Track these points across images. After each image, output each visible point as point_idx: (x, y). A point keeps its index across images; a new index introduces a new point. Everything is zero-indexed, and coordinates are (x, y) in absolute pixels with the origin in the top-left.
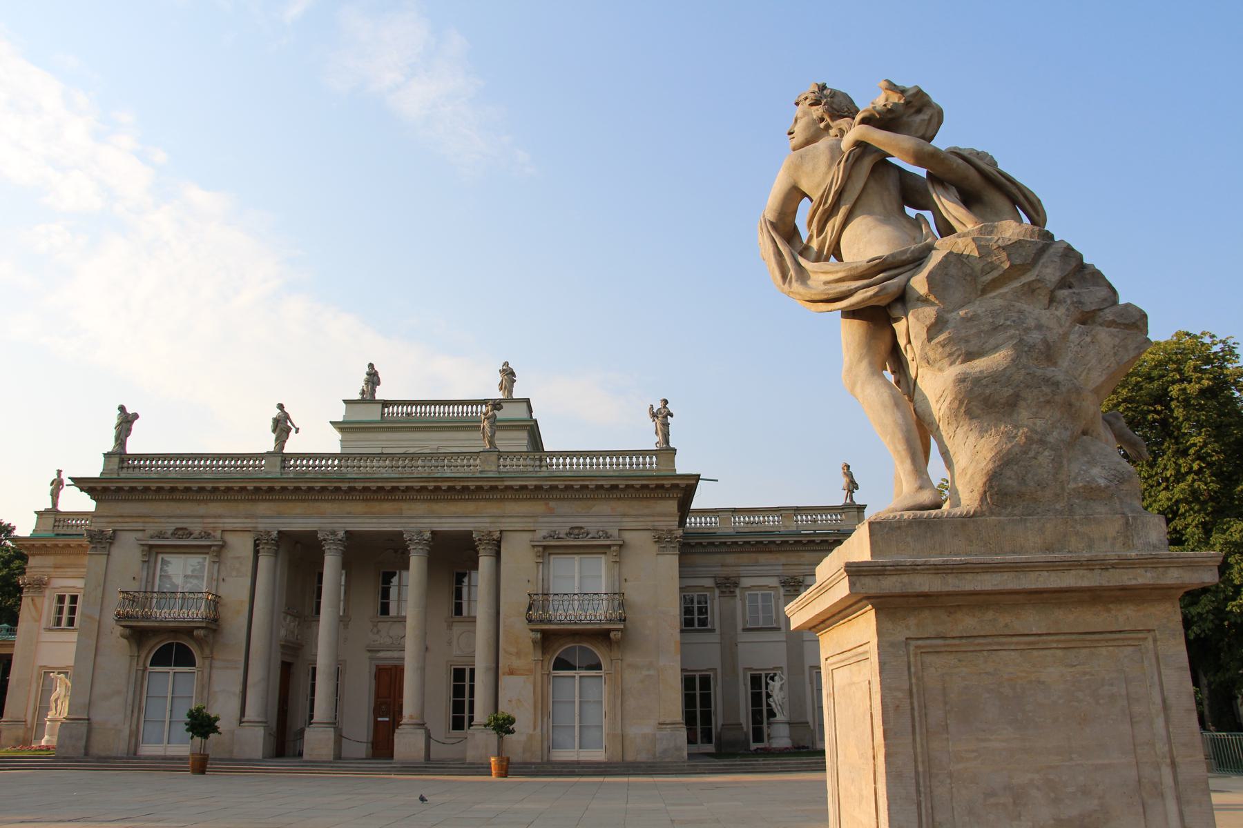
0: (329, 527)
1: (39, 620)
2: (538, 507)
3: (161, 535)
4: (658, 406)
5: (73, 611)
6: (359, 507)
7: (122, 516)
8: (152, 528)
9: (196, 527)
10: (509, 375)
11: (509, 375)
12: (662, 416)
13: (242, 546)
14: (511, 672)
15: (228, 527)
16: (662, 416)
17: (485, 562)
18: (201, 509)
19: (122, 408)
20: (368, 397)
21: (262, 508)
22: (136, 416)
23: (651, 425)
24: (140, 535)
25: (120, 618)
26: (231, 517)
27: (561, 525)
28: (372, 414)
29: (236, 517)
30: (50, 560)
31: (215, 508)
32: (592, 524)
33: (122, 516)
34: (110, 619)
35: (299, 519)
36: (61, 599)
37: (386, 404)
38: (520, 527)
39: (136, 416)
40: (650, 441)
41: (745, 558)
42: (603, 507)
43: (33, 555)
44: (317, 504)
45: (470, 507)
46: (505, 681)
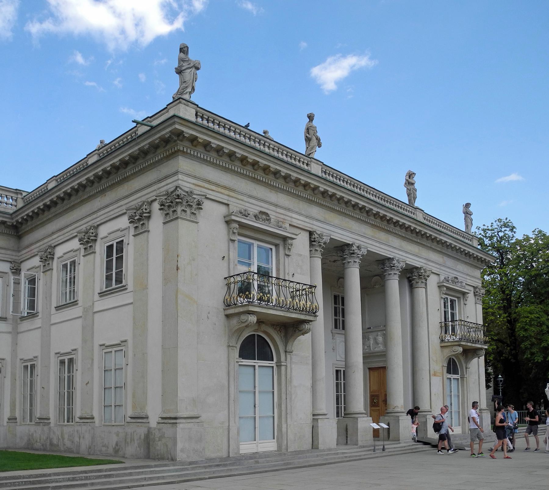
0: (357, 243)
3: (246, 215)
7: (209, 182)
15: (295, 222)
26: (297, 213)
29: (300, 214)
33: (209, 182)
44: (347, 220)
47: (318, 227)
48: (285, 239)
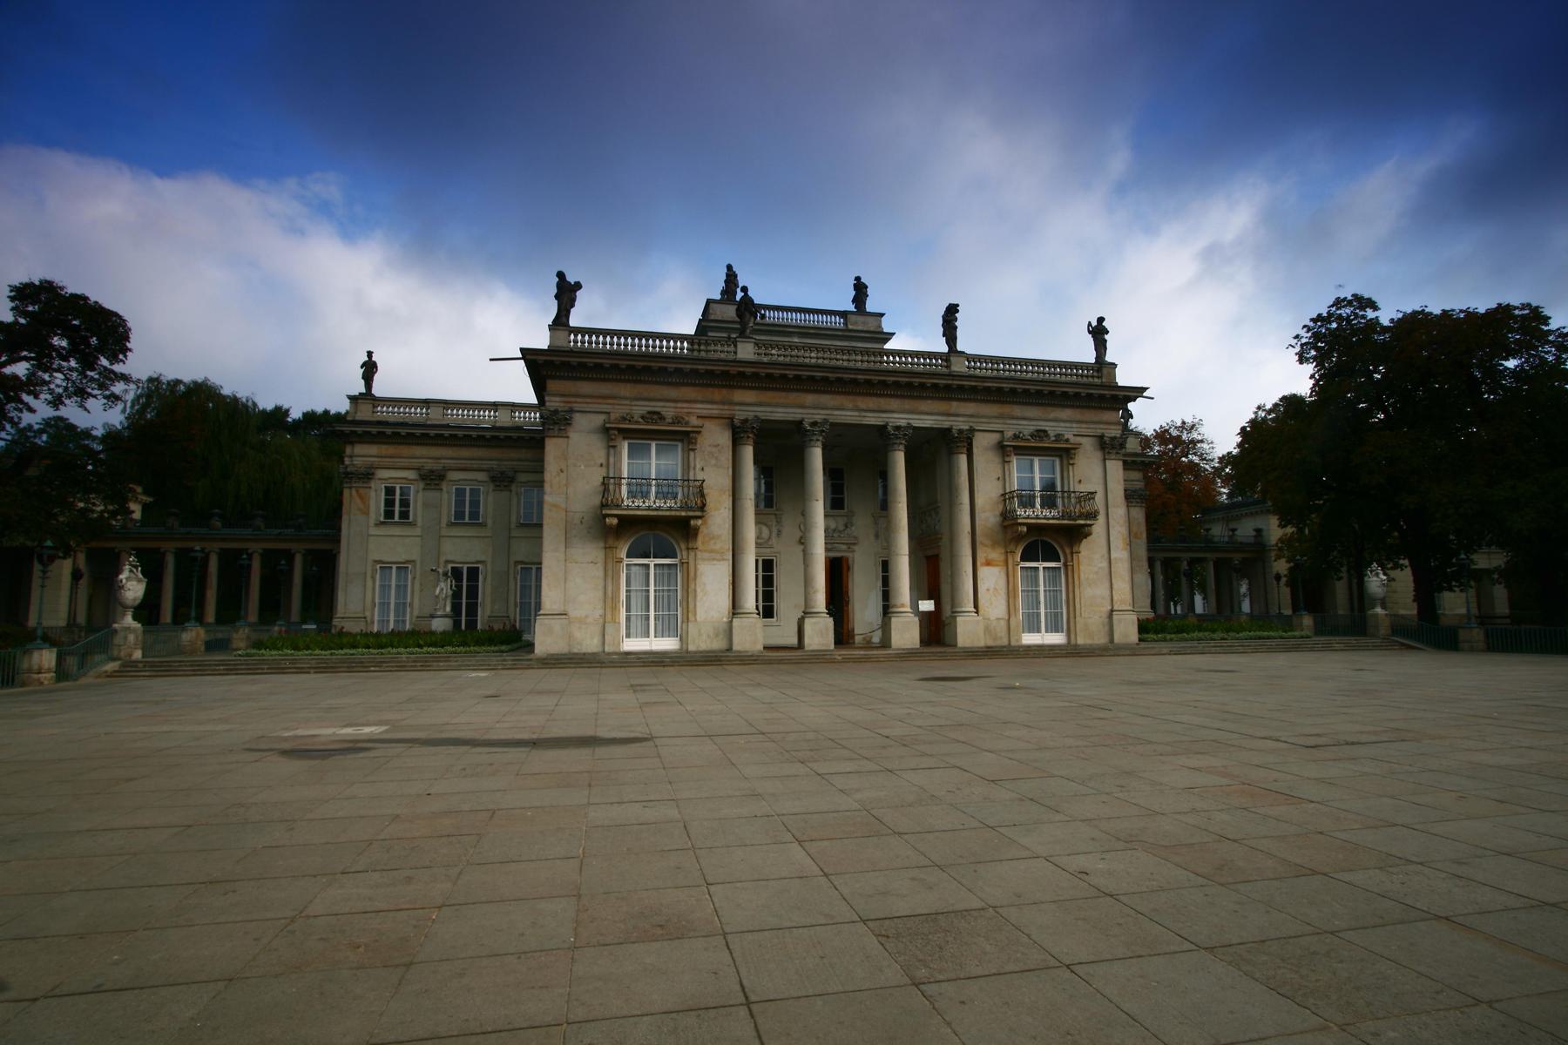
1: (366, 513)
4: (1094, 323)
8: (618, 411)
9: (669, 411)
10: (860, 289)
11: (860, 289)
12: (1098, 332)
14: (988, 563)
15: (705, 412)
16: (1098, 332)
18: (672, 392)
19: (561, 275)
21: (739, 395)
22: (578, 286)
23: (1089, 341)
24: (602, 417)
27: (1027, 428)
30: (373, 450)
32: (1052, 429)
35: (782, 409)
38: (987, 426)
39: (578, 286)
40: (1089, 357)
43: (352, 443)
46: (984, 572)
47: (741, 414)
48: (687, 433)
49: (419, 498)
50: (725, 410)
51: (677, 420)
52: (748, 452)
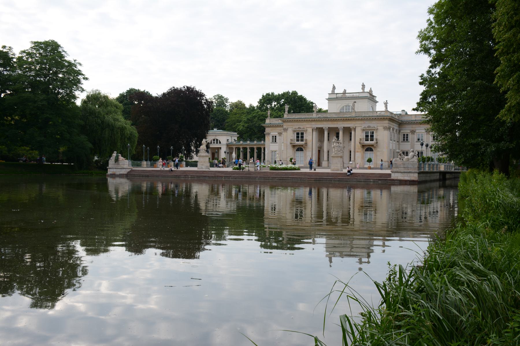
2: (362, 122)
5: (275, 139)
6: (330, 123)
8: (294, 127)
9: (302, 127)
13: (310, 130)
17: (353, 133)
20: (333, 93)
21: (313, 123)
23: (384, 105)
25: (291, 143)
28: (334, 96)
31: (305, 123)
32: (372, 125)
34: (289, 143)
35: (320, 125)
36: (273, 137)
37: (337, 94)
41: (417, 126)
42: (374, 122)
45: (350, 122)
46: (356, 153)
49: (277, 138)
50: (311, 126)
51: (304, 128)
52: (314, 133)
